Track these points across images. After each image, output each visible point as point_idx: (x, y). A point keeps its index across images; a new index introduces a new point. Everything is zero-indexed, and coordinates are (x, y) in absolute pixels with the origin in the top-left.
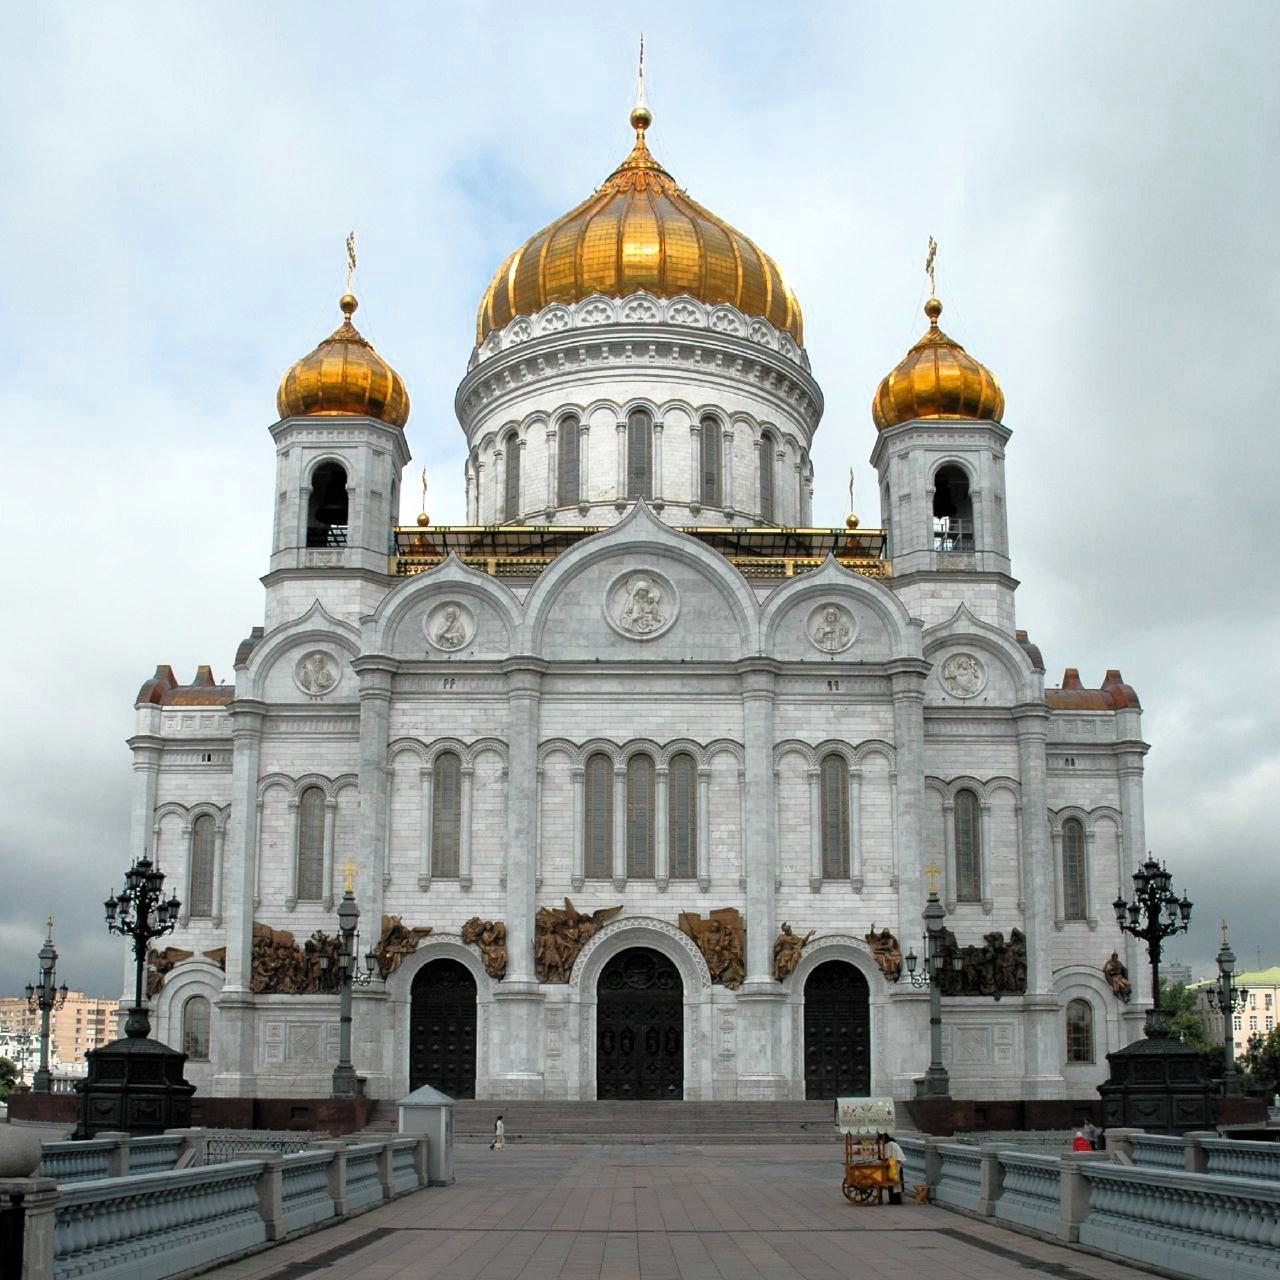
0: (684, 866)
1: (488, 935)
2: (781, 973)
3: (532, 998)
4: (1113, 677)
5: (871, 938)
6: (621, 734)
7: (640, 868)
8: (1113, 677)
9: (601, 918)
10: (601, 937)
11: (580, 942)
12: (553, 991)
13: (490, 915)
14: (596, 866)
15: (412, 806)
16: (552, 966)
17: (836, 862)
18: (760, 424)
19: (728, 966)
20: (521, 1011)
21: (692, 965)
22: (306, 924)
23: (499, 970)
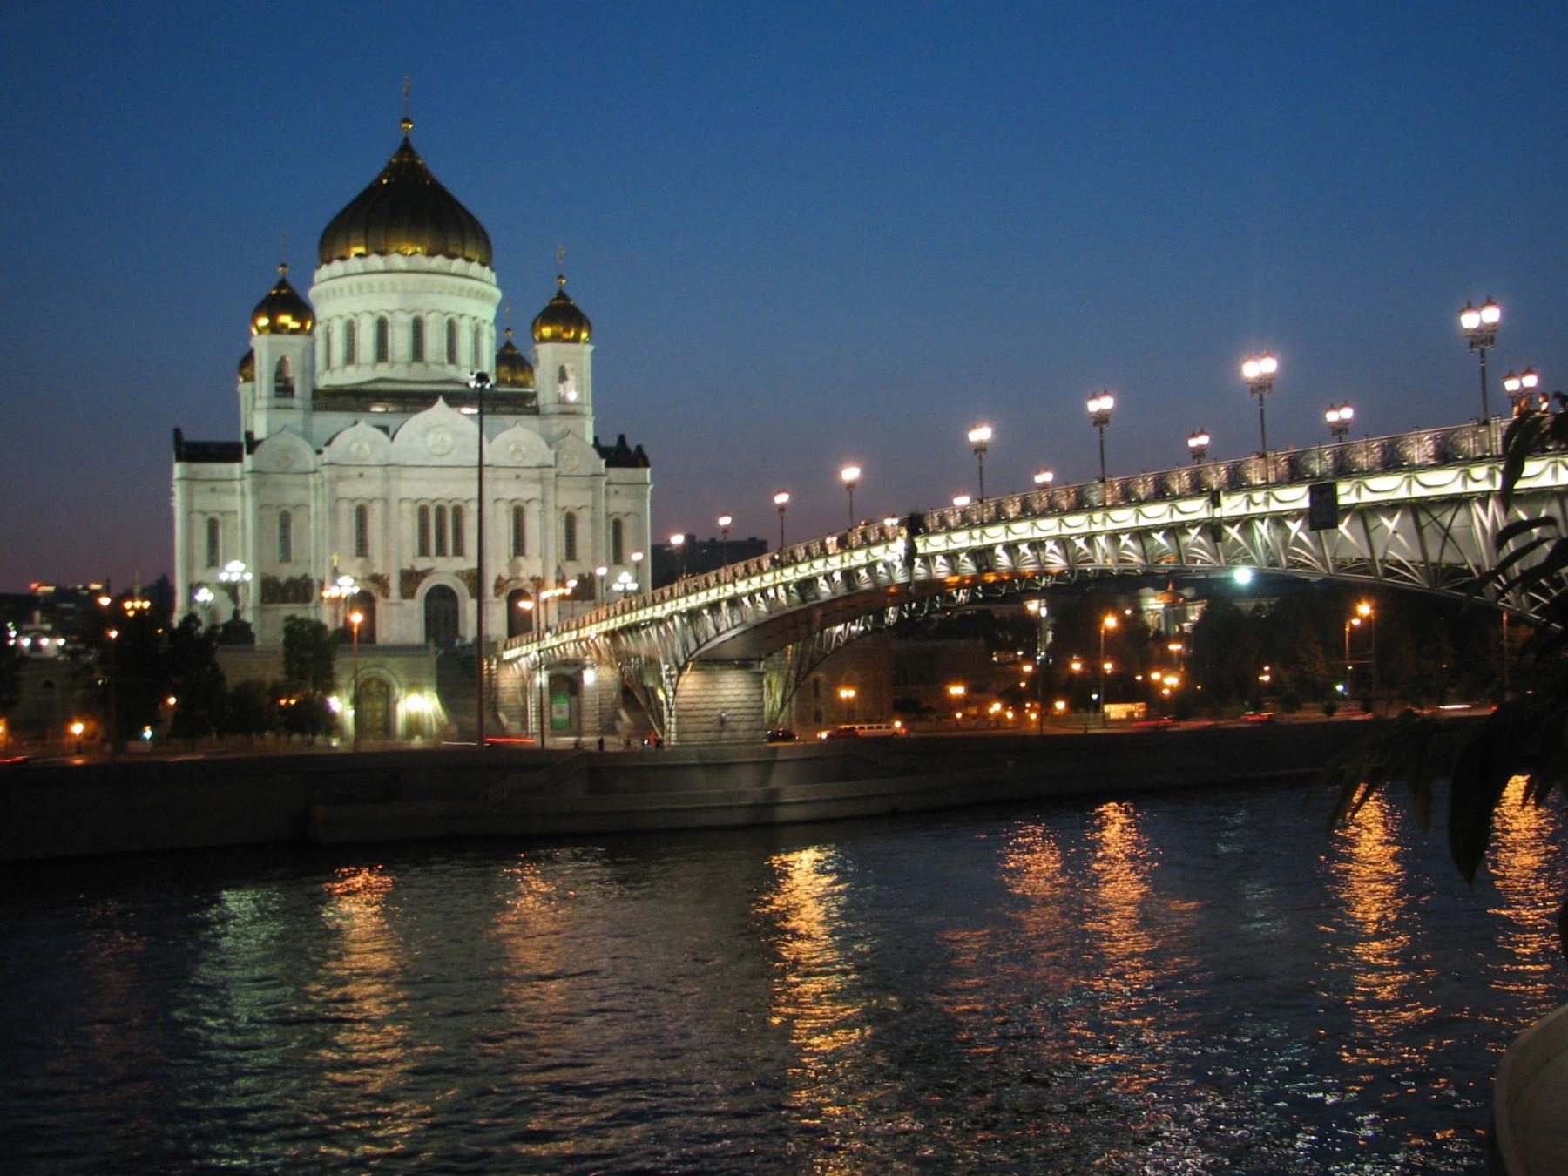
0: (459, 551)
1: (379, 581)
2: (497, 595)
3: (399, 604)
4: (639, 448)
5: (533, 579)
6: (434, 496)
7: (441, 551)
8: (639, 448)
9: (424, 574)
10: (426, 580)
11: (418, 584)
12: (408, 602)
13: (378, 570)
14: (424, 551)
15: (347, 527)
16: (408, 592)
17: (519, 547)
18: (474, 318)
19: (478, 591)
20: (395, 609)
21: (461, 589)
22: (286, 573)
23: (386, 595)
